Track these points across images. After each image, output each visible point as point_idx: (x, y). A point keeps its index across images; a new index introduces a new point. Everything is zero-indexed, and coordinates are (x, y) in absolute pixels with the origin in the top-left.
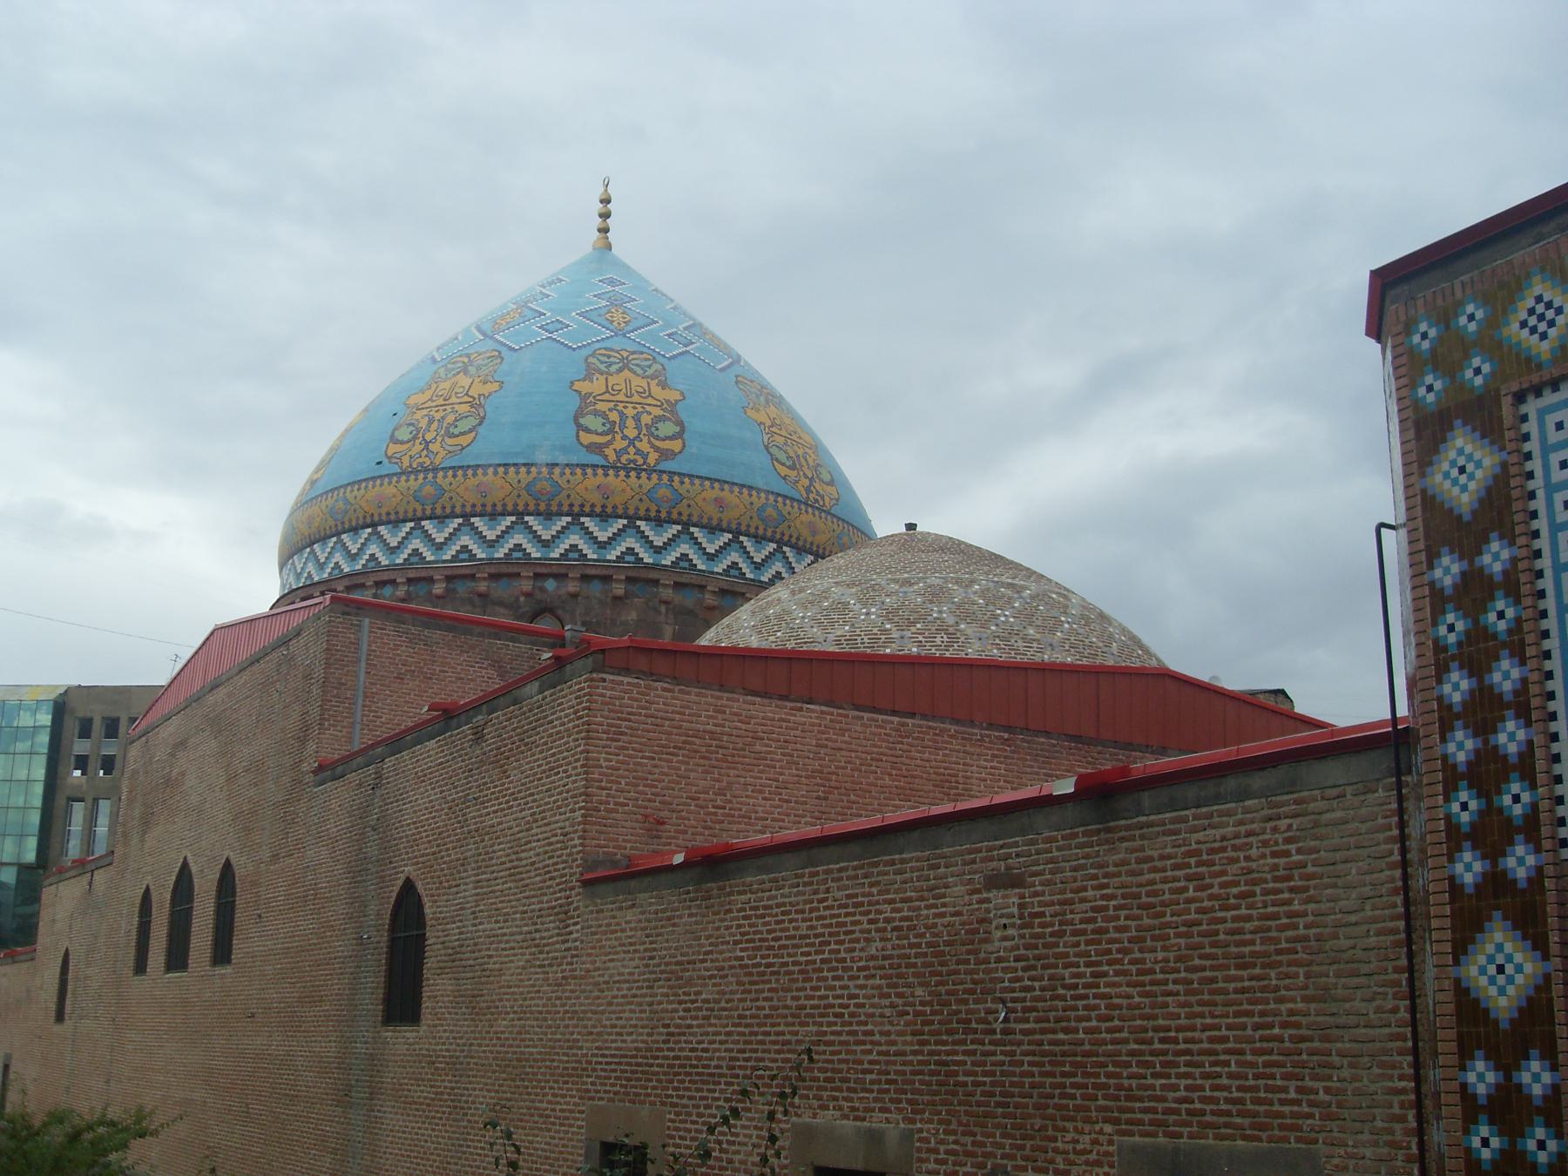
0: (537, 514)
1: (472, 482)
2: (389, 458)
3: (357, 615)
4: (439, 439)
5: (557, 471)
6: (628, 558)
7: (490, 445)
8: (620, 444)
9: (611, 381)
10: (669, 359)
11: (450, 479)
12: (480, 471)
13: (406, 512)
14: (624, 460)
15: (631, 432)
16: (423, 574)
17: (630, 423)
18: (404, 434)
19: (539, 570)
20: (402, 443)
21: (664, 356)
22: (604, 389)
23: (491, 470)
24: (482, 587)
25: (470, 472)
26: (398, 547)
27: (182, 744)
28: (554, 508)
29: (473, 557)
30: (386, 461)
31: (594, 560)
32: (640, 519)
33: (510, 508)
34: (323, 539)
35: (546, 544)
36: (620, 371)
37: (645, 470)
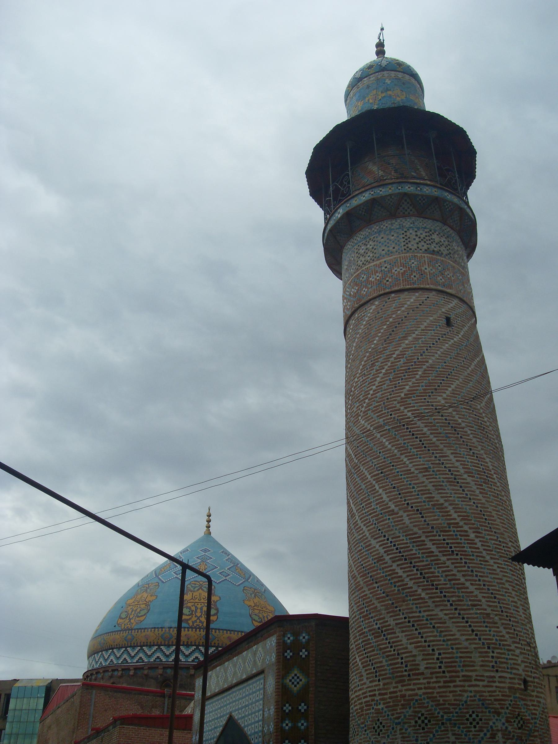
0: (165, 645)
1: (144, 634)
2: (118, 624)
3: (91, 689)
4: (134, 618)
5: (172, 630)
6: (195, 660)
7: (150, 620)
8: (194, 619)
9: (194, 594)
10: (218, 583)
11: (136, 633)
12: (146, 630)
13: (122, 645)
14: (195, 625)
15: (198, 614)
16: (127, 667)
17: (199, 610)
18: (123, 616)
19: (165, 666)
20: (123, 619)
21: (216, 582)
22: (191, 598)
23: (150, 630)
24: (146, 672)
25: (143, 631)
26: (119, 657)
27: (49, 727)
28: (170, 643)
29: (143, 661)
30: (117, 625)
31: (184, 662)
32: (201, 646)
33: (156, 643)
34: (98, 653)
35: (167, 656)
36: (198, 590)
37: (202, 628)
